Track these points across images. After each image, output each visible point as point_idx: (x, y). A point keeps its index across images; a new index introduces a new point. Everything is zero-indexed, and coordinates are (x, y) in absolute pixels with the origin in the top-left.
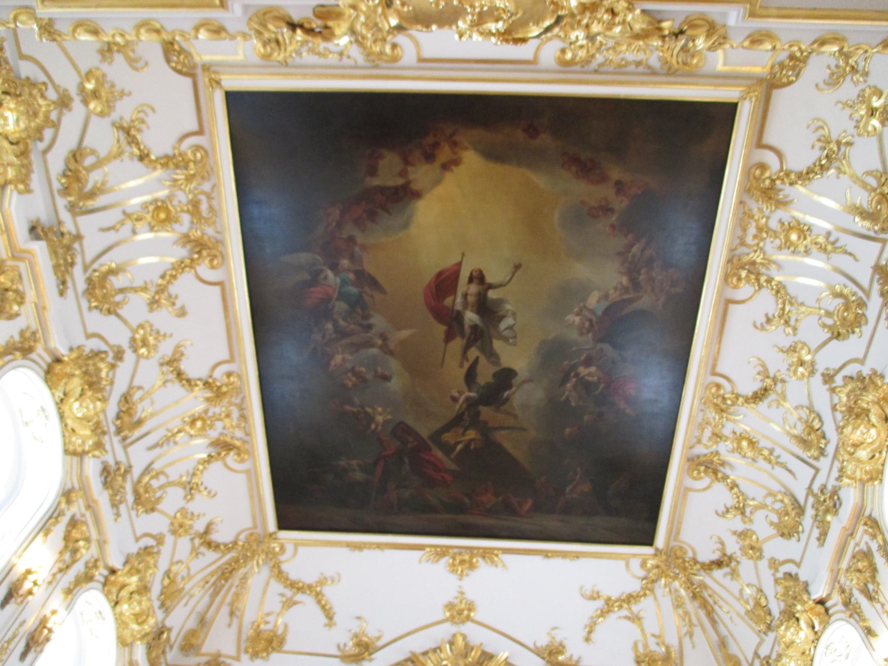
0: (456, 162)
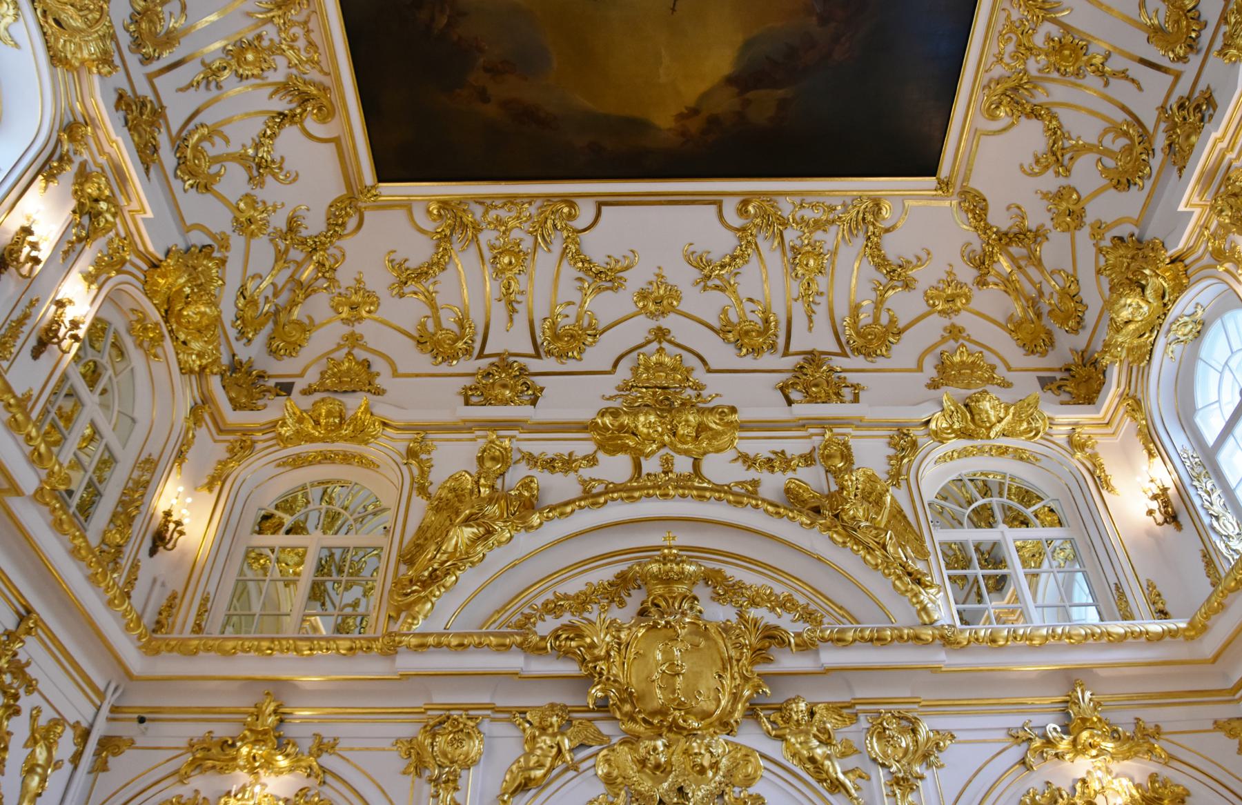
0: (681, 117)
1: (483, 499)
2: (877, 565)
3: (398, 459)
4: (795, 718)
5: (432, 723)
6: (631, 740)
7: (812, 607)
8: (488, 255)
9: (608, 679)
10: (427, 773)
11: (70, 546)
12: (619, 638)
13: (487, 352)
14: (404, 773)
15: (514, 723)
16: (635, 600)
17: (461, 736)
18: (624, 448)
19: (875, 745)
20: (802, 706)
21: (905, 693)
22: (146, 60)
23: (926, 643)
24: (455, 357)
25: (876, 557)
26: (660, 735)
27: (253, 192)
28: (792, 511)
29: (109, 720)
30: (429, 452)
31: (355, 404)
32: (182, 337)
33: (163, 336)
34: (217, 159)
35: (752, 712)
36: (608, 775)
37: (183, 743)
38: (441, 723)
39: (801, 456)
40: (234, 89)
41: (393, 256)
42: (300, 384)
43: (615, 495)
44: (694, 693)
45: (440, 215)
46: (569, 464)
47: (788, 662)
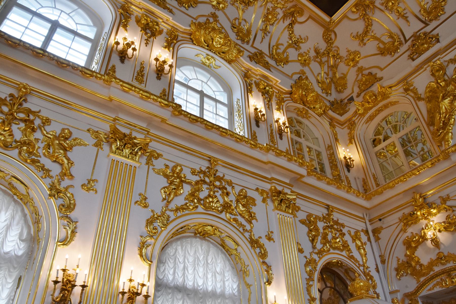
1: (444, 87)
3: (403, 95)
8: (382, 8)
11: (326, 182)
13: (407, 38)
22: (248, 42)
24: (398, 48)
27: (299, 52)
29: (370, 224)
30: (412, 85)
31: (376, 88)
32: (312, 107)
33: (307, 110)
34: (284, 51)
37: (398, 220)
40: (273, 29)
41: (353, 35)
42: (354, 95)
45: (357, 10)
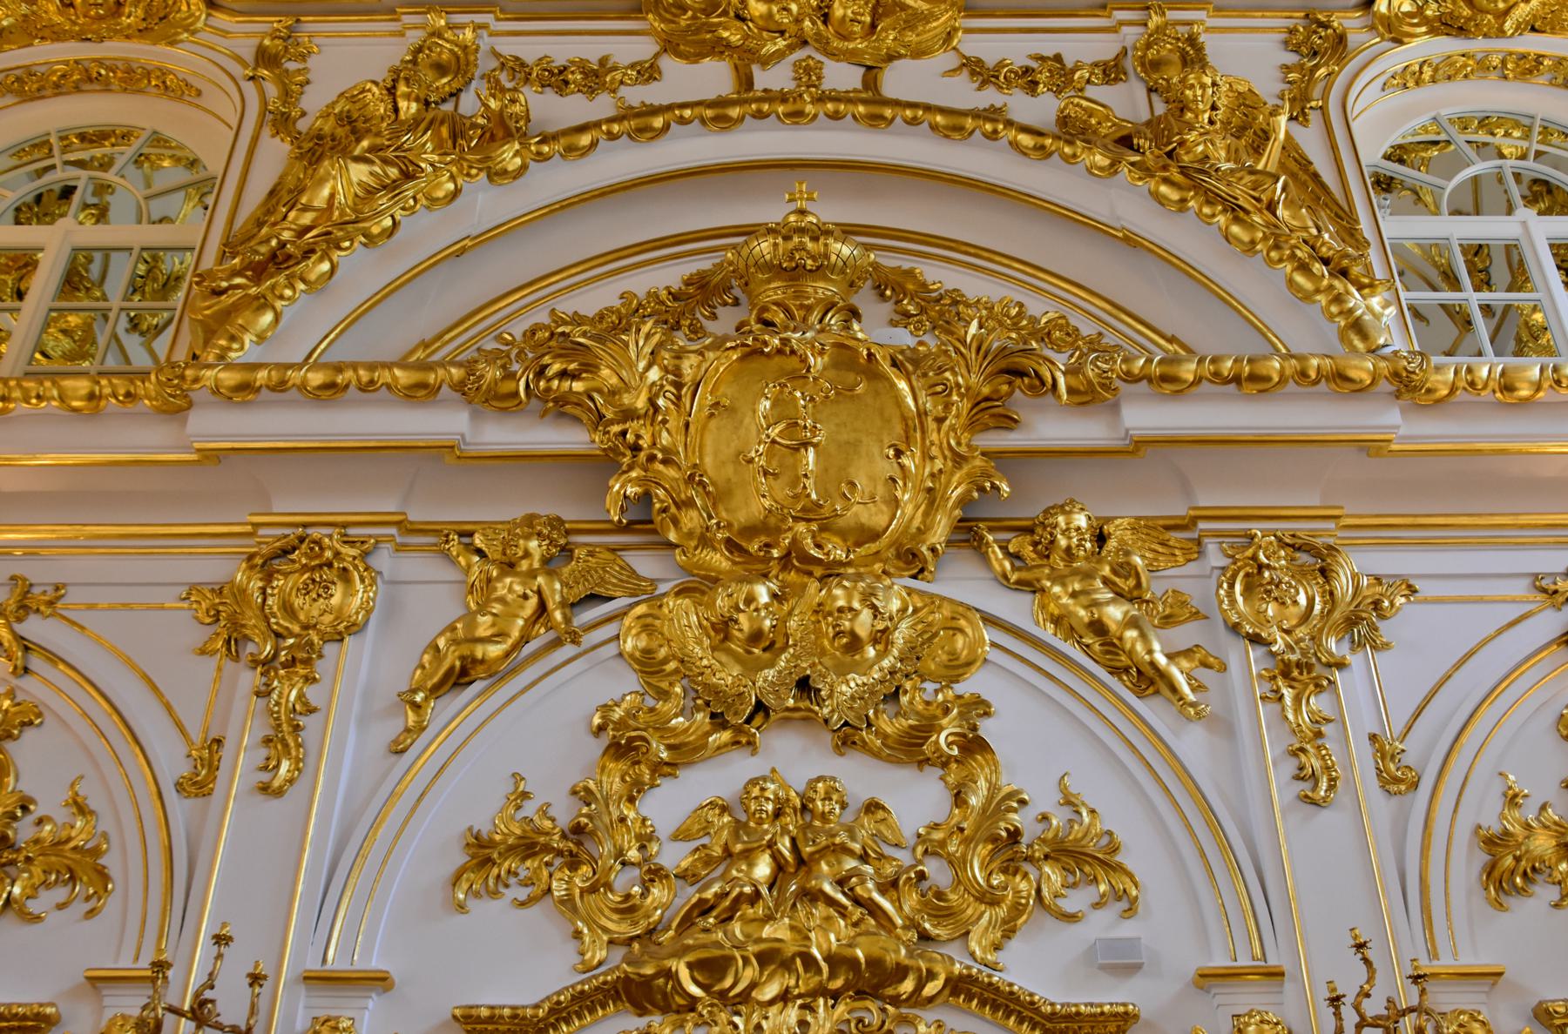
1: (403, 123)
2: (1253, 242)
3: (237, 70)
4: (1063, 542)
5: (265, 550)
6: (698, 586)
7: (1110, 339)
9: (651, 458)
10: (250, 648)
12: (677, 372)
14: (203, 652)
15: (446, 555)
16: (725, 321)
17: (327, 574)
18: (718, 48)
19: (1240, 599)
20: (1081, 520)
21: (1309, 499)
23: (1360, 390)
25: (1251, 227)
26: (766, 576)
28: (1070, 143)
35: (967, 534)
36: (647, 652)
38: (285, 552)
39: (1096, 65)
43: (687, 113)
44: (839, 480)
46: (595, 77)
47: (1049, 427)
